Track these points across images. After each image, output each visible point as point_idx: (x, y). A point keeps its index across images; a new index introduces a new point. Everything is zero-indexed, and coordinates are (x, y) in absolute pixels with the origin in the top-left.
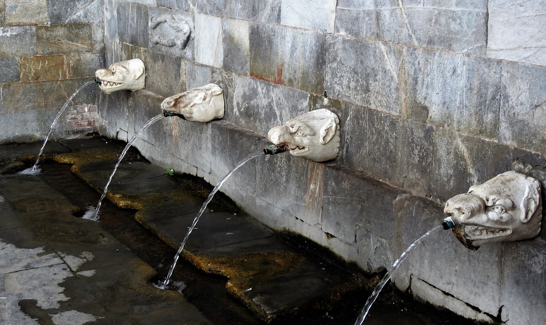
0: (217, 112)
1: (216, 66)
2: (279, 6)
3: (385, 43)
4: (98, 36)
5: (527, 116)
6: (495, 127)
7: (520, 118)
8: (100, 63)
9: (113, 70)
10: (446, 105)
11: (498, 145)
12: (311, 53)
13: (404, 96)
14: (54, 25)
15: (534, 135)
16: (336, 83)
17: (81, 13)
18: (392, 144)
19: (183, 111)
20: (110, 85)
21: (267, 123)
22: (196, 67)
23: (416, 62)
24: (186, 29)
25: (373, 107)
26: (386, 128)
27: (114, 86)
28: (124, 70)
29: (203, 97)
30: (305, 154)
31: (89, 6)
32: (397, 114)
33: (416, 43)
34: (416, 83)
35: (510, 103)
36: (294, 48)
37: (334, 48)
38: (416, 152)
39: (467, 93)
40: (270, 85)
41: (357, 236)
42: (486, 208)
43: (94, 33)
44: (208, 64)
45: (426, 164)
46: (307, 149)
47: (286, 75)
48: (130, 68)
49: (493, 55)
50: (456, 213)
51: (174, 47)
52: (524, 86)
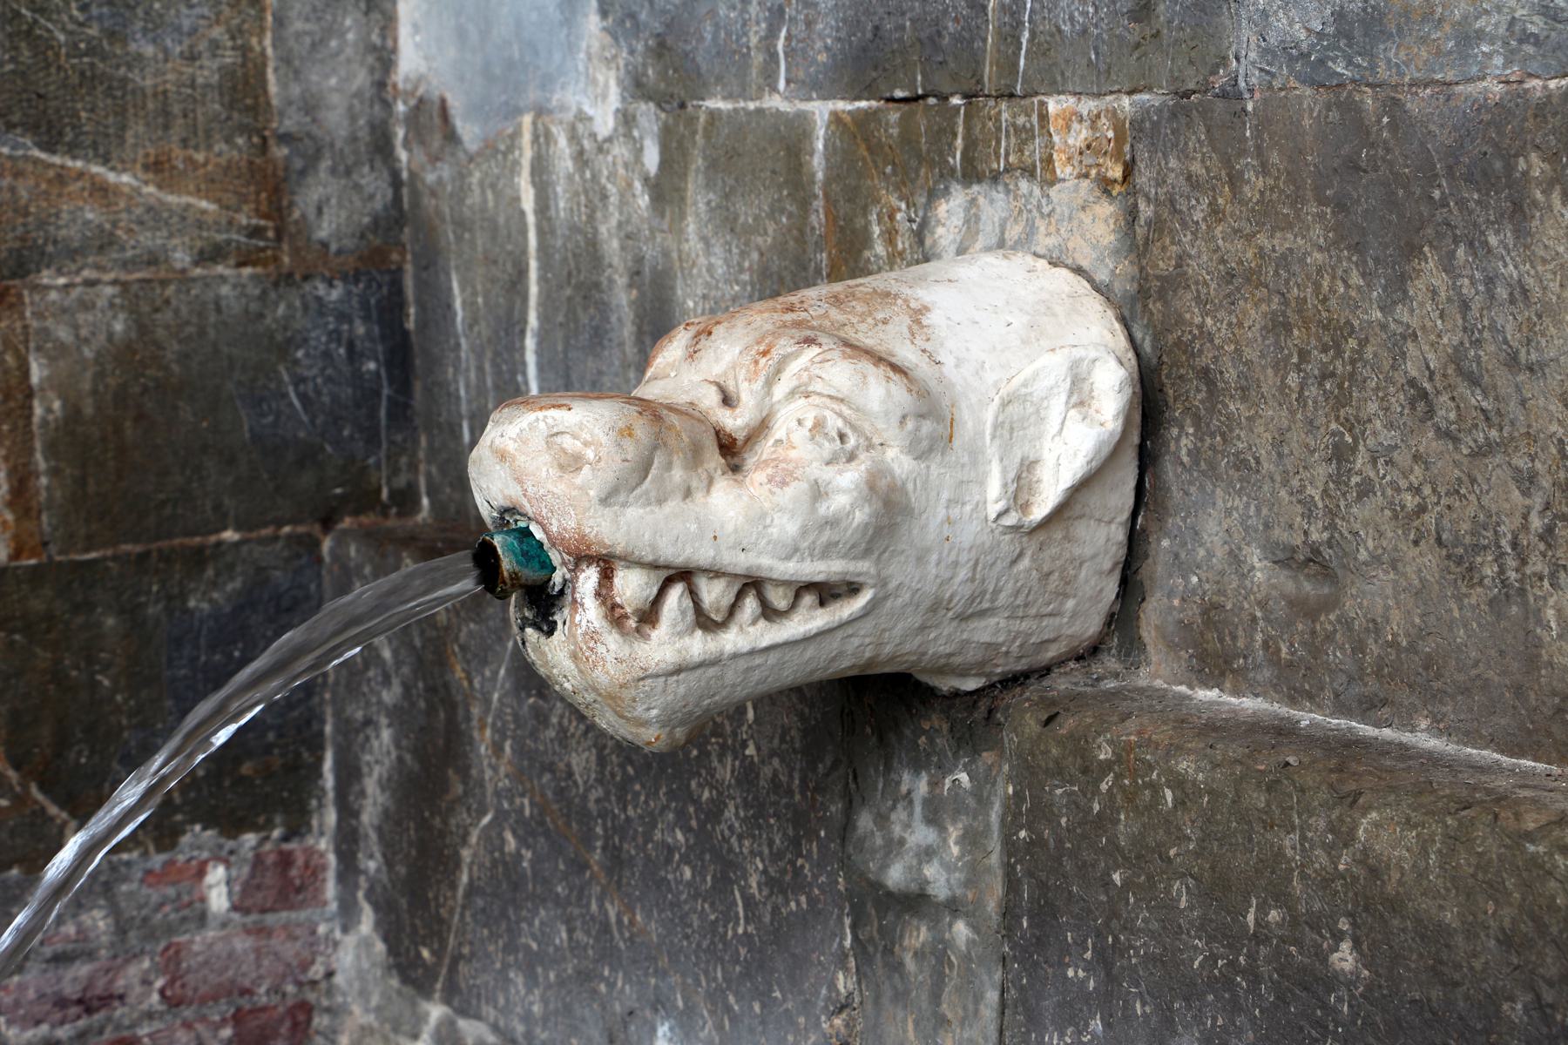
9: (727, 400)
20: (704, 621)
48: (949, 369)
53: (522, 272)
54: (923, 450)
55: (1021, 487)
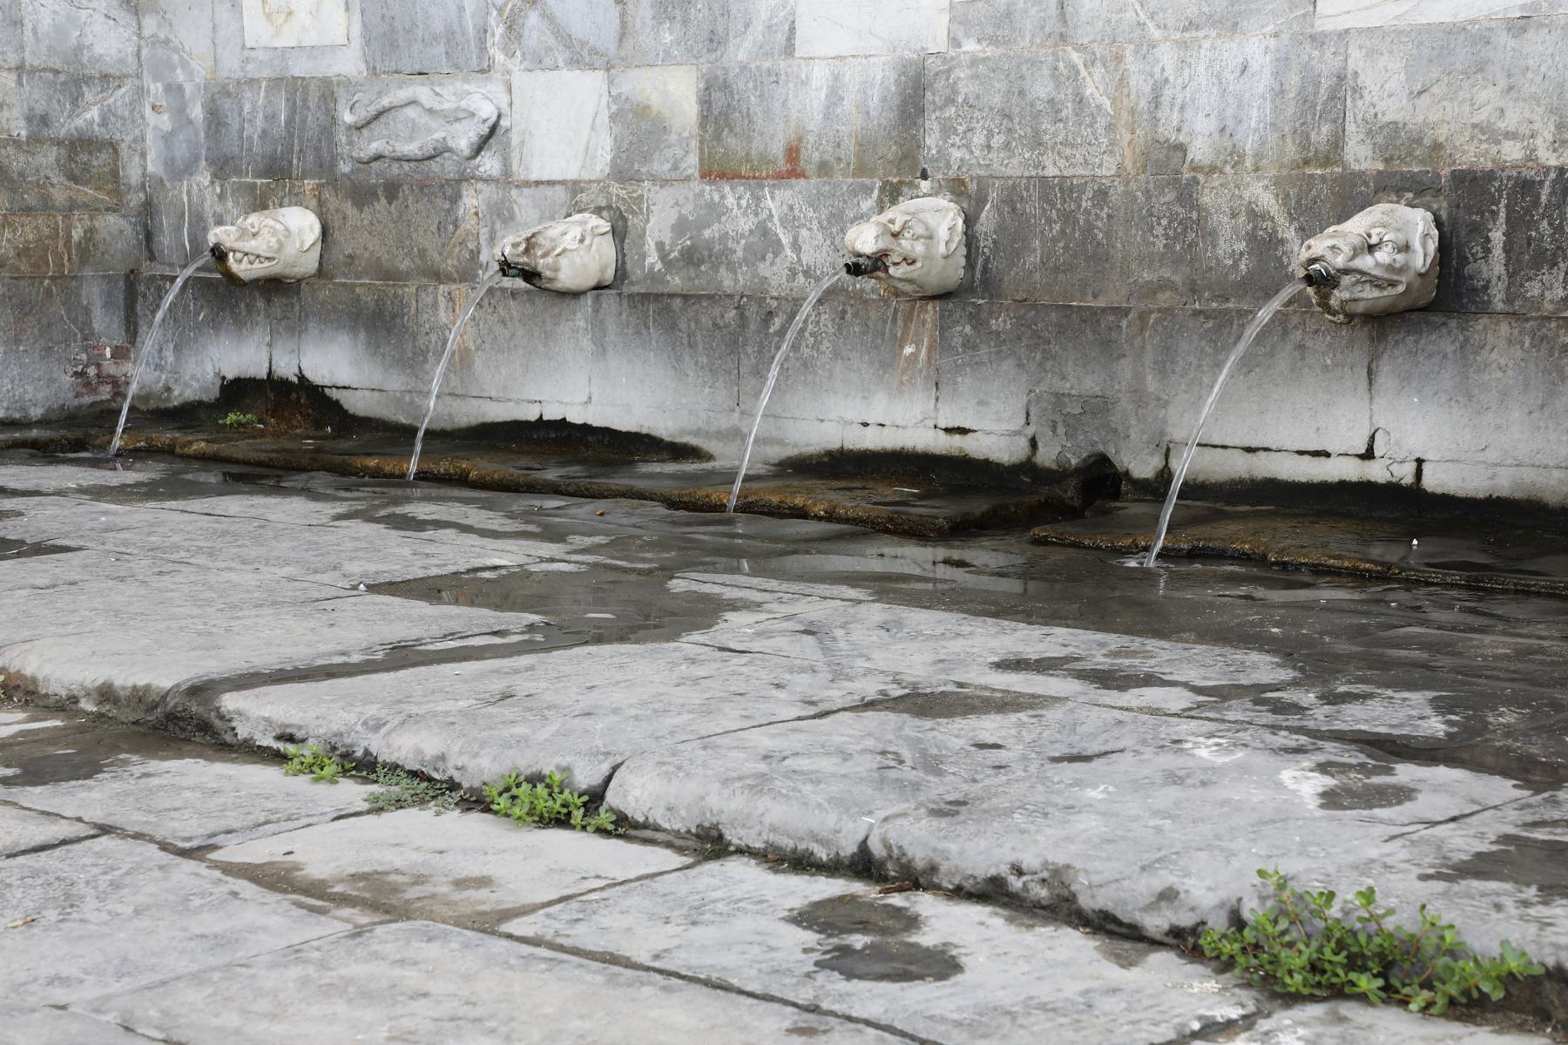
0: (603, 271)
1: (586, 176)
2: (791, 19)
3: (1081, 48)
4: (133, 173)
5: (1402, 113)
6: (1337, 147)
7: (1388, 118)
8: (138, 240)
9: (253, 227)
10: (1228, 132)
11: (1342, 176)
12: (884, 99)
13: (1127, 137)
14: (35, 140)
15: (1419, 141)
16: (953, 145)
17: (94, 114)
18: (1100, 230)
19: (542, 264)
21: (753, 265)
22: (514, 192)
23: (1157, 70)
24: (487, 111)
25: (1051, 171)
26: (1084, 204)
27: (257, 265)
28: (278, 226)
29: (579, 237)
30: (915, 275)
31: (112, 100)
32: (1112, 172)
33: (1156, 34)
34: (1156, 107)
35: (1367, 98)
36: (835, 96)
37: (948, 79)
38: (1159, 231)
39: (1273, 100)
40: (762, 187)
41: (1032, 414)
42: (1371, 248)
43: (123, 167)
44: (555, 177)
45: (1182, 248)
46: (919, 265)
47: (811, 156)
49: (1324, 25)
50: (1329, 256)
51: (438, 159)
52: (1396, 65)
53: (183, 214)
54: (286, 237)
55: (302, 246)
